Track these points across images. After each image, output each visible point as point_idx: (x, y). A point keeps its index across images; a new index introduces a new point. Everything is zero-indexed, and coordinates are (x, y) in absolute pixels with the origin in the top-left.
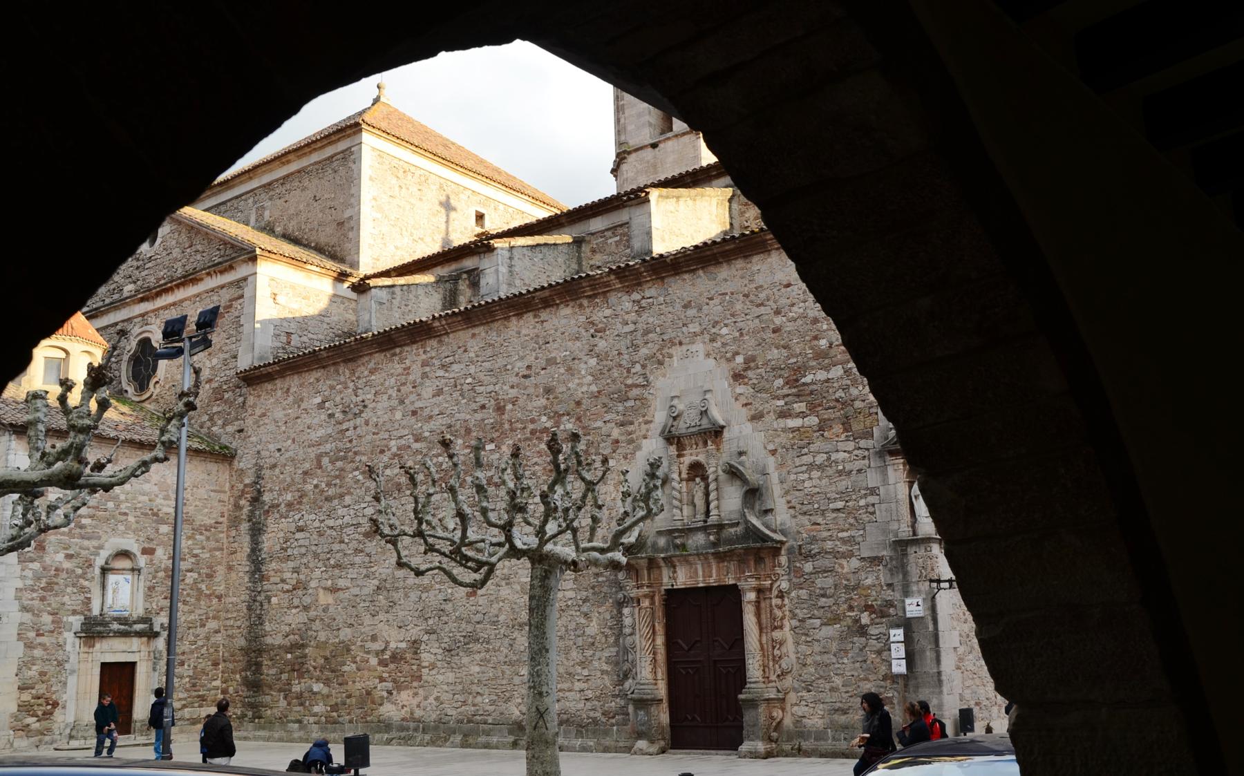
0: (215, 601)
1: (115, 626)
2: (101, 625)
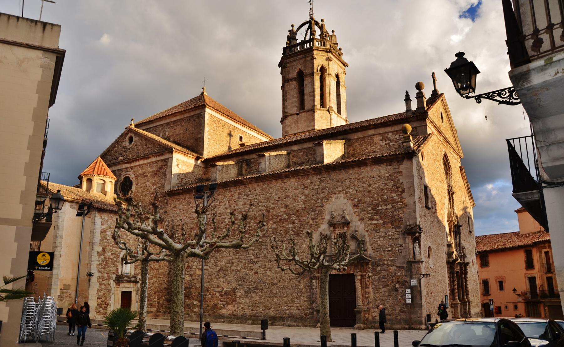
0: (155, 271)
1: (126, 279)
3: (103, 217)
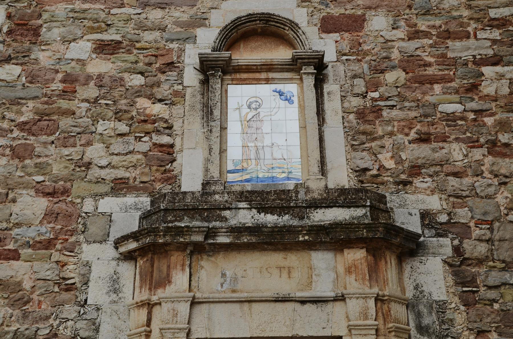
2: (193, 211)
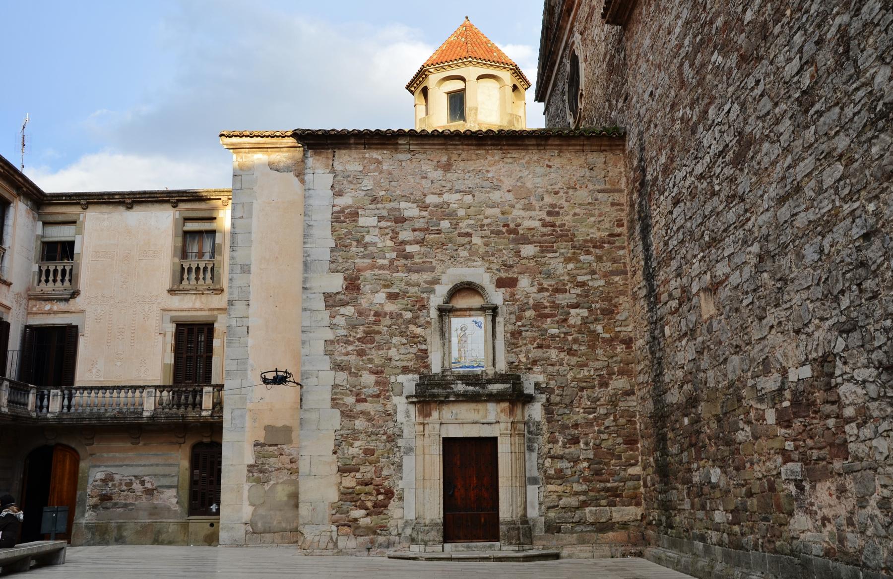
0: (620, 348)
1: (460, 387)
2: (438, 385)
3: (338, 167)
